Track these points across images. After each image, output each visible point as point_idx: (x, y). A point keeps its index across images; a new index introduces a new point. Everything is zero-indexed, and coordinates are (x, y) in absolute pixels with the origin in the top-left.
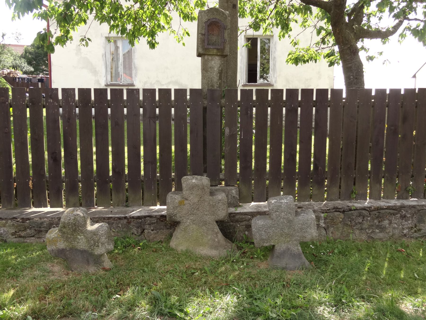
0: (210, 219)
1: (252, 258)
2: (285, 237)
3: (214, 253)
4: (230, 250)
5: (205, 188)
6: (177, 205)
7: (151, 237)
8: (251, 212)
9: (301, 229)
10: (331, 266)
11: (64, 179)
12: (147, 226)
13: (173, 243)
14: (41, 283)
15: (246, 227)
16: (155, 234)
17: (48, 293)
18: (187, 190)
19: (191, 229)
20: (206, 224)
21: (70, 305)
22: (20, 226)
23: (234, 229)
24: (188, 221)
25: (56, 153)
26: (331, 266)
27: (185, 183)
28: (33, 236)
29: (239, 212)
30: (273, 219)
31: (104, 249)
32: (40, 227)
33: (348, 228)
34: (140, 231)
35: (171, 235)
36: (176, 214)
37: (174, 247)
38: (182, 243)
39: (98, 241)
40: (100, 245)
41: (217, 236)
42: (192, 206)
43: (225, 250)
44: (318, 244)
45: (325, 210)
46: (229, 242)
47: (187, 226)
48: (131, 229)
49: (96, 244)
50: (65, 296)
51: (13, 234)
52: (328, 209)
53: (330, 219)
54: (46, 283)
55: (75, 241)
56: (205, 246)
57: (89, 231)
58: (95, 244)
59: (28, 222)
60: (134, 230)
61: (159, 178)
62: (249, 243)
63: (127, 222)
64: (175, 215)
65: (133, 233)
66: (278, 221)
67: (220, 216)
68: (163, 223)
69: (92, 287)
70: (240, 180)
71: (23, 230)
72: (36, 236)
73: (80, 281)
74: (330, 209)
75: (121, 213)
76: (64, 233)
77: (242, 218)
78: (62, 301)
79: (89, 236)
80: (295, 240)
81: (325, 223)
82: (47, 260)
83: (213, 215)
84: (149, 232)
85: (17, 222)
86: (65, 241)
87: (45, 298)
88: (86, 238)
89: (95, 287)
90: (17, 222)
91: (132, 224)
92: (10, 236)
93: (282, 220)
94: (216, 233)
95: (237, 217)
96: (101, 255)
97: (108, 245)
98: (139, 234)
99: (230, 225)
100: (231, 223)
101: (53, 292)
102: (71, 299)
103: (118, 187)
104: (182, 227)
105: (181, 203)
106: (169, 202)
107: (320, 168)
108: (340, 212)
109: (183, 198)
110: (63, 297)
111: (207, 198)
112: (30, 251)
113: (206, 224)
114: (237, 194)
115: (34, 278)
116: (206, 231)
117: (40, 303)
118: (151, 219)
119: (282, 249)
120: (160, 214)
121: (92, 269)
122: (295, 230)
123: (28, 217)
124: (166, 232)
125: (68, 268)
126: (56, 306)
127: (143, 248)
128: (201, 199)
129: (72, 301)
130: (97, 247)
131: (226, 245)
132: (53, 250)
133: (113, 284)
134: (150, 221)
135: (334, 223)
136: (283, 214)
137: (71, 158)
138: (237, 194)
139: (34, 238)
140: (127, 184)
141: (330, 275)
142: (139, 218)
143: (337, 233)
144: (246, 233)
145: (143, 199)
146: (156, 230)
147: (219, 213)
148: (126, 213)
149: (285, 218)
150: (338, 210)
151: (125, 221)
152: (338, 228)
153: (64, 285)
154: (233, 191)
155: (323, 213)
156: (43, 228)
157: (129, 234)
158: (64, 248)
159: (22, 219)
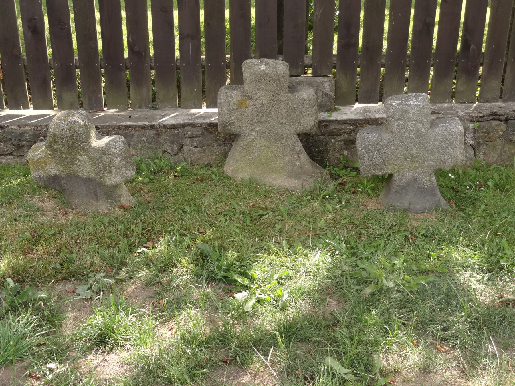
0: (290, 130)
1: (354, 193)
2: (411, 161)
3: (293, 184)
4: (319, 179)
6: (235, 108)
7: (194, 158)
8: (355, 120)
9: (439, 148)
10: (483, 207)
11: (52, 64)
12: (187, 141)
13: (229, 168)
14: (25, 227)
15: (345, 144)
16: (200, 152)
17: (36, 243)
18: (251, 83)
19: (258, 146)
20: (282, 138)
21: (72, 262)
23: (326, 146)
24: (253, 133)
25: (35, 19)
26: (483, 207)
27: (249, 71)
28: (11, 154)
29: (335, 119)
30: (392, 132)
31: (119, 177)
32: (20, 140)
33: (511, 146)
34: (176, 147)
35: (225, 155)
36: (234, 122)
37: (230, 173)
38: (243, 168)
39: (110, 164)
40: (114, 171)
41: (299, 157)
42: (260, 110)
43: (312, 180)
44: (461, 172)
45: (477, 117)
46: (318, 168)
47: (250, 142)
48: (162, 144)
49: (108, 168)
50: (64, 248)
52: (482, 115)
53: (484, 132)
54: (33, 228)
55: (73, 164)
56: (280, 172)
57: (94, 148)
58: (105, 169)
60: (167, 147)
61: (204, 63)
62: (349, 169)
63: (155, 134)
64: (232, 124)
65: (165, 151)
66: (402, 136)
67: (305, 125)
68: (212, 135)
69: (104, 234)
70: (338, 67)
72: (15, 153)
73: (85, 224)
74: (483, 116)
75: (146, 118)
76: (56, 151)
77: (340, 130)
78: (58, 255)
79: (96, 155)
80: (427, 166)
81: (474, 138)
82: (34, 192)
83: (293, 124)
84: (190, 150)
86: (57, 163)
87: (32, 250)
88: (91, 159)
89: (108, 235)
91: (163, 136)
93: (407, 133)
94: (298, 153)
95: (332, 127)
96: (116, 186)
98: (176, 152)
100: (322, 137)
101: (45, 241)
102: (72, 252)
103: (140, 77)
104: (242, 142)
105: (241, 104)
106: (221, 103)
107: (472, 46)
108: (501, 121)
109: (245, 96)
110: (60, 250)
111: (285, 95)
112: (6, 177)
113: (282, 138)
114: (331, 91)
115: (15, 219)
116: (281, 149)
117: (25, 258)
118: (193, 129)
119: (404, 180)
120: (207, 121)
121: (103, 207)
122: (428, 151)
124: (218, 149)
125: (66, 205)
126: (49, 263)
127: (182, 175)
128: (275, 98)
129: (74, 256)
130: (108, 173)
131: (313, 172)
132: (40, 177)
133: (137, 230)
134: (192, 132)
135: (490, 138)
136: (410, 123)
137: (61, 29)
138: (331, 91)
139: (12, 157)
140: (153, 72)
141: (480, 222)
142: (173, 127)
143: (492, 154)
144: (346, 152)
145: (179, 97)
146: (201, 147)
147: (304, 120)
148: (153, 119)
149: (413, 131)
150: (497, 117)
151: (152, 132)
152: (494, 146)
153: (61, 231)
154: (326, 85)
155: (472, 121)
156: (25, 141)
157: (159, 153)
158: (58, 174)
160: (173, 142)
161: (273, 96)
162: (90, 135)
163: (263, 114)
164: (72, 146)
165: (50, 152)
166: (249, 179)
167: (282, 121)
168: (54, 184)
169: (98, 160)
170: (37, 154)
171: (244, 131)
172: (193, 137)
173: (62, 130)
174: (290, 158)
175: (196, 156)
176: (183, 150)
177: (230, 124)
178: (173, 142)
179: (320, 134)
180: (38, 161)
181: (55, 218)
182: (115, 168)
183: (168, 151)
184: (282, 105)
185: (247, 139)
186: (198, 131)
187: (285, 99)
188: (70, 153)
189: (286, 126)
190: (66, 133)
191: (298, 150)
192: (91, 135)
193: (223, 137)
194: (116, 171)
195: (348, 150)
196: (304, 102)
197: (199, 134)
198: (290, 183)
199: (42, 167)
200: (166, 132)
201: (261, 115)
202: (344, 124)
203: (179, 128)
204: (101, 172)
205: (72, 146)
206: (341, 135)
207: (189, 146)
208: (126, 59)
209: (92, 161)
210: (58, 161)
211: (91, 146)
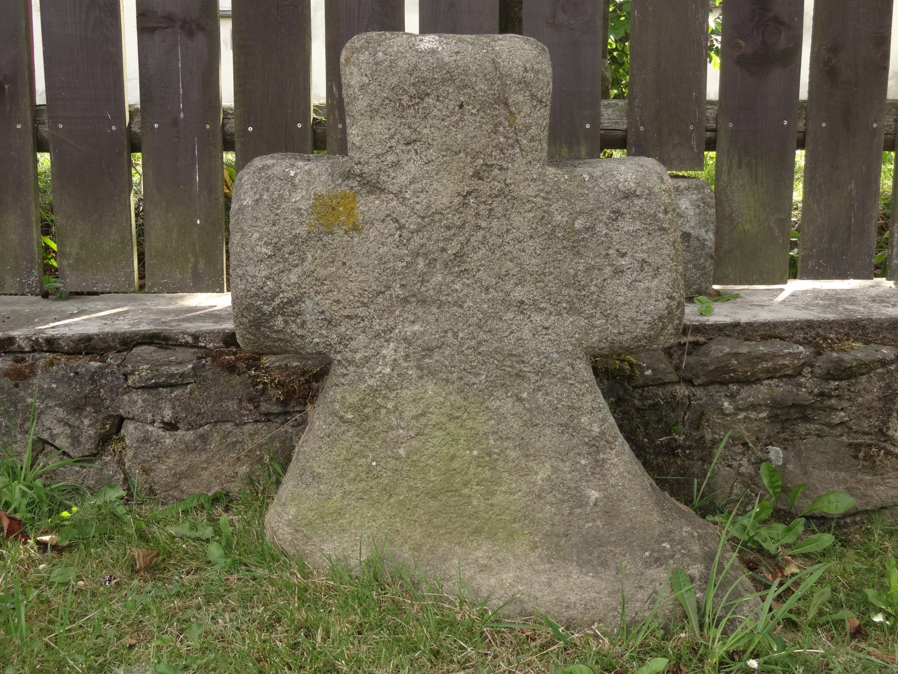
0: (555, 338)
1: (859, 633)
4: (696, 570)
5: (517, 97)
6: (302, 230)
7: (163, 472)
12: (134, 403)
13: (281, 519)
15: (774, 418)
16: (189, 449)
18: (373, 112)
20: (519, 375)
24: (388, 351)
29: (728, 320)
34: (88, 428)
36: (299, 300)
38: (340, 512)
41: (600, 464)
42: (417, 240)
43: (661, 574)
46: (682, 514)
47: (375, 391)
48: (30, 414)
56: (511, 535)
60: (53, 424)
62: (799, 525)
64: (290, 307)
67: (625, 315)
68: (236, 380)
70: (722, 142)
83: (572, 310)
84: (145, 440)
91: (40, 381)
94: (595, 446)
95: (721, 349)
98: (88, 446)
99: (674, 403)
100: (682, 390)
104: (337, 394)
105: (329, 214)
106: (241, 209)
109: (348, 175)
111: (530, 172)
113: (519, 375)
114: (703, 224)
116: (516, 425)
118: (161, 355)
124: (255, 435)
128: (485, 187)
134: (155, 366)
138: (703, 224)
142: (87, 346)
144: (776, 453)
146: (191, 427)
147: (618, 291)
160: (77, 408)
161: (477, 175)
163: (431, 263)
166: (369, 563)
167: (518, 294)
171: (344, 340)
172: (157, 386)
174: (555, 470)
175: (170, 462)
176: (122, 439)
177: (281, 309)
179: (673, 377)
183: (57, 443)
184: (521, 221)
185: (361, 379)
186: (181, 362)
187: (531, 191)
189: (538, 318)
191: (596, 429)
193: (281, 384)
195: (784, 444)
196: (622, 206)
197: (182, 375)
198: (560, 583)
200: (52, 364)
201: (421, 263)
202: (765, 338)
203: (109, 349)
206: (758, 381)
207: (144, 422)
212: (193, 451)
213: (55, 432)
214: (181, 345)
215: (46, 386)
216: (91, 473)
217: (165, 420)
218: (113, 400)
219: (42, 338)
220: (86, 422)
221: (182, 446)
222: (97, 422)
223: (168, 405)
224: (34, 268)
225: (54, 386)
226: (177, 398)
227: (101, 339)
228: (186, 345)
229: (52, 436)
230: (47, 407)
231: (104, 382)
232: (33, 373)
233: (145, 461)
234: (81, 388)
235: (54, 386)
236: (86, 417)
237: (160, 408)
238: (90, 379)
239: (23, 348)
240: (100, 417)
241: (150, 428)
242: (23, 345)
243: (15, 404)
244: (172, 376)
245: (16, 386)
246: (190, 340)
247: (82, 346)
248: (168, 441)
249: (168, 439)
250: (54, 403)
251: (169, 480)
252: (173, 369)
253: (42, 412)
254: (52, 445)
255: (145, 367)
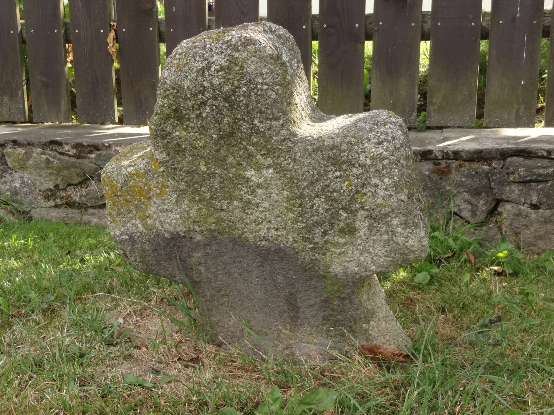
7: (526, 235)
12: (514, 192)
16: (546, 221)
22: (67, 168)
31: (379, 250)
34: (483, 205)
39: (353, 201)
40: (362, 224)
51: (49, 195)
55: (231, 197)
57: (304, 140)
58: (334, 216)
59: (93, 156)
60: (461, 203)
63: (434, 172)
65: (455, 214)
71: (80, 183)
76: (178, 150)
79: (306, 167)
84: (519, 215)
85: (62, 154)
86: (181, 194)
88: (290, 182)
90: (62, 154)
91: (455, 176)
92: (41, 200)
96: (359, 282)
97: (406, 224)
98: (481, 217)
118: (528, 162)
121: (311, 348)
123: (96, 141)
125: (205, 329)
130: (342, 232)
132: (132, 240)
140: (425, 47)
142: (478, 156)
151: (427, 167)
159: (78, 146)
160: (476, 193)
162: (291, 96)
164: (231, 134)
165: (161, 156)
168: (165, 259)
169: (312, 183)
170: (127, 163)
172: (530, 181)
173: (203, 70)
175: (533, 229)
176: (500, 214)
178: (476, 193)
180: (126, 183)
181: (157, 372)
182: (370, 217)
183: (463, 214)
188: (224, 159)
190: (216, 82)
192: (297, 100)
194: (370, 228)
197: (547, 175)
199: (136, 207)
200: (460, 166)
203: (493, 158)
204: (319, 230)
205: (231, 134)
207: (518, 203)
208: (369, 16)
209: (290, 189)
210: (183, 185)
211: (294, 135)
212: (548, 222)
213: (461, 208)
214: (538, 157)
215: (459, 179)
216: (481, 234)
217: (533, 203)
218: (499, 189)
219: (451, 151)
220: (482, 202)
221: (542, 219)
222: (487, 202)
223: (535, 193)
224: (414, 111)
225: (464, 179)
226: (541, 190)
227: (488, 152)
228: (543, 157)
229: (460, 210)
230: (459, 192)
231: (495, 178)
232: (450, 171)
233: (517, 228)
234: (480, 181)
235: (464, 179)
236: (482, 199)
237: (530, 195)
238: (485, 176)
239: (437, 157)
240: (490, 199)
241: (522, 208)
242: (438, 155)
243: (439, 190)
244: (541, 175)
245: (441, 179)
246: (545, 154)
247: (476, 156)
248: (533, 215)
249: (533, 215)
250: (463, 190)
251: (531, 240)
252: (541, 171)
253: (455, 195)
254: (458, 215)
255: (522, 169)
